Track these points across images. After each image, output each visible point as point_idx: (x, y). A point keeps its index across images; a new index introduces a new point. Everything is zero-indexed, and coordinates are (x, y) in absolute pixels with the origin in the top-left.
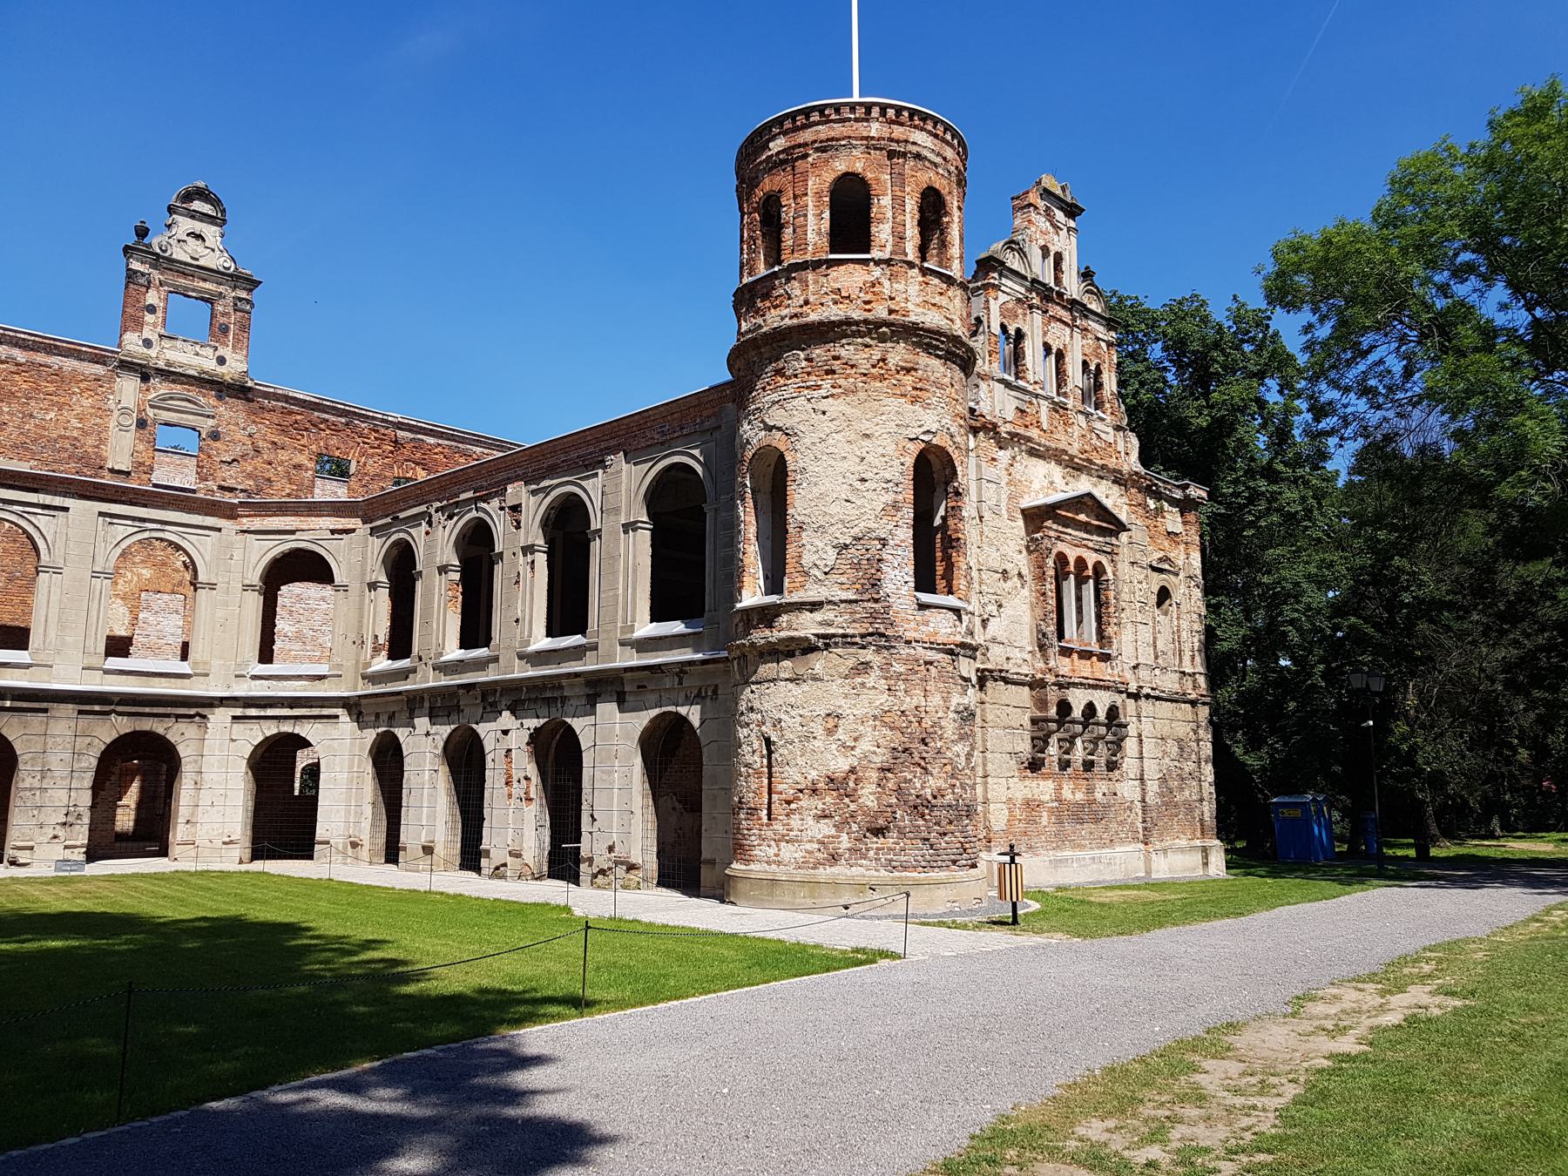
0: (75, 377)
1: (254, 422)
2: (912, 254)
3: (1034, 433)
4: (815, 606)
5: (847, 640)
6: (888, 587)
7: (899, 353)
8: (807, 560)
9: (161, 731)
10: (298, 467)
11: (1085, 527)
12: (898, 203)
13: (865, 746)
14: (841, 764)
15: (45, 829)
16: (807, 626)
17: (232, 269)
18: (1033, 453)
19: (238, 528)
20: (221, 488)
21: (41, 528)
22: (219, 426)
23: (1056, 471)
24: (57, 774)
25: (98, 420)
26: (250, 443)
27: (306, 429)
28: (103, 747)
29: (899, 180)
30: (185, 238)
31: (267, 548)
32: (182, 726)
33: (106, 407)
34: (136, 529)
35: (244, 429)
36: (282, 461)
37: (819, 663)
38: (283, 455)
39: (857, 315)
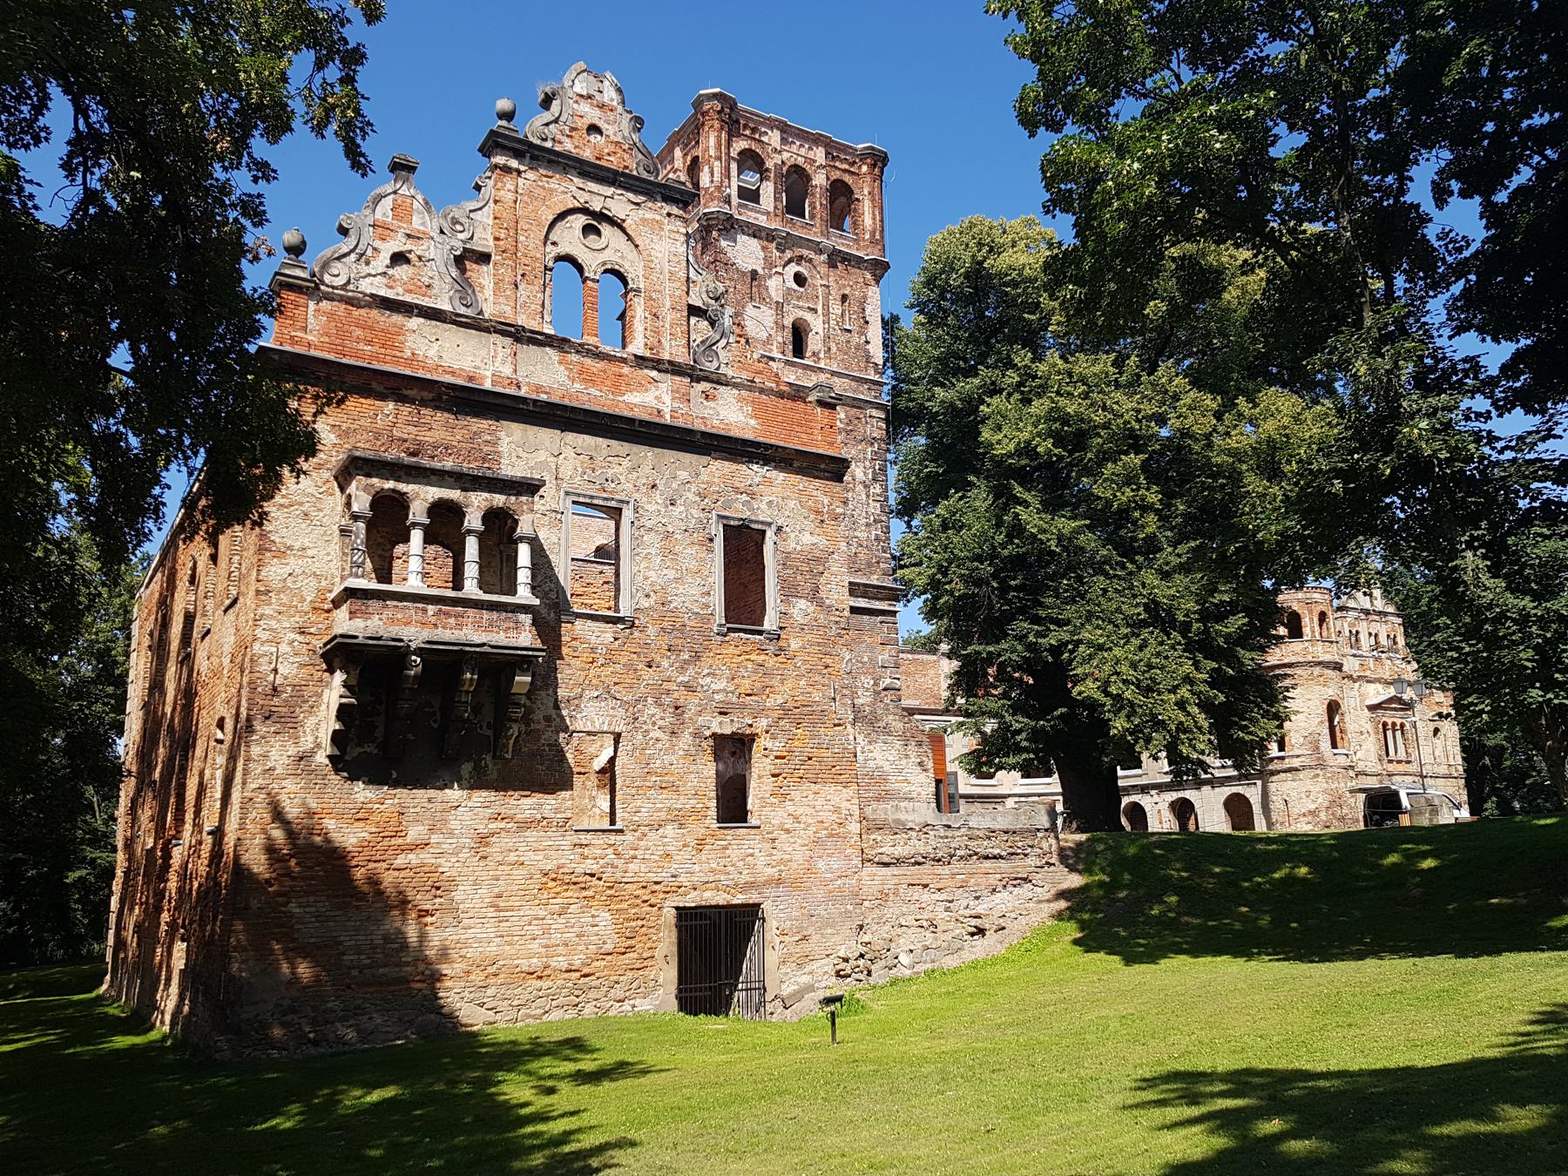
2: (1318, 638)
3: (1368, 673)
4: (1298, 756)
5: (1311, 767)
6: (1322, 749)
7: (1317, 670)
8: (1293, 742)
11: (1395, 709)
12: (1311, 620)
13: (1320, 800)
14: (1313, 807)
16: (1296, 763)
18: (1368, 682)
23: (1379, 687)
29: (1311, 612)
37: (1301, 775)
39: (1301, 660)
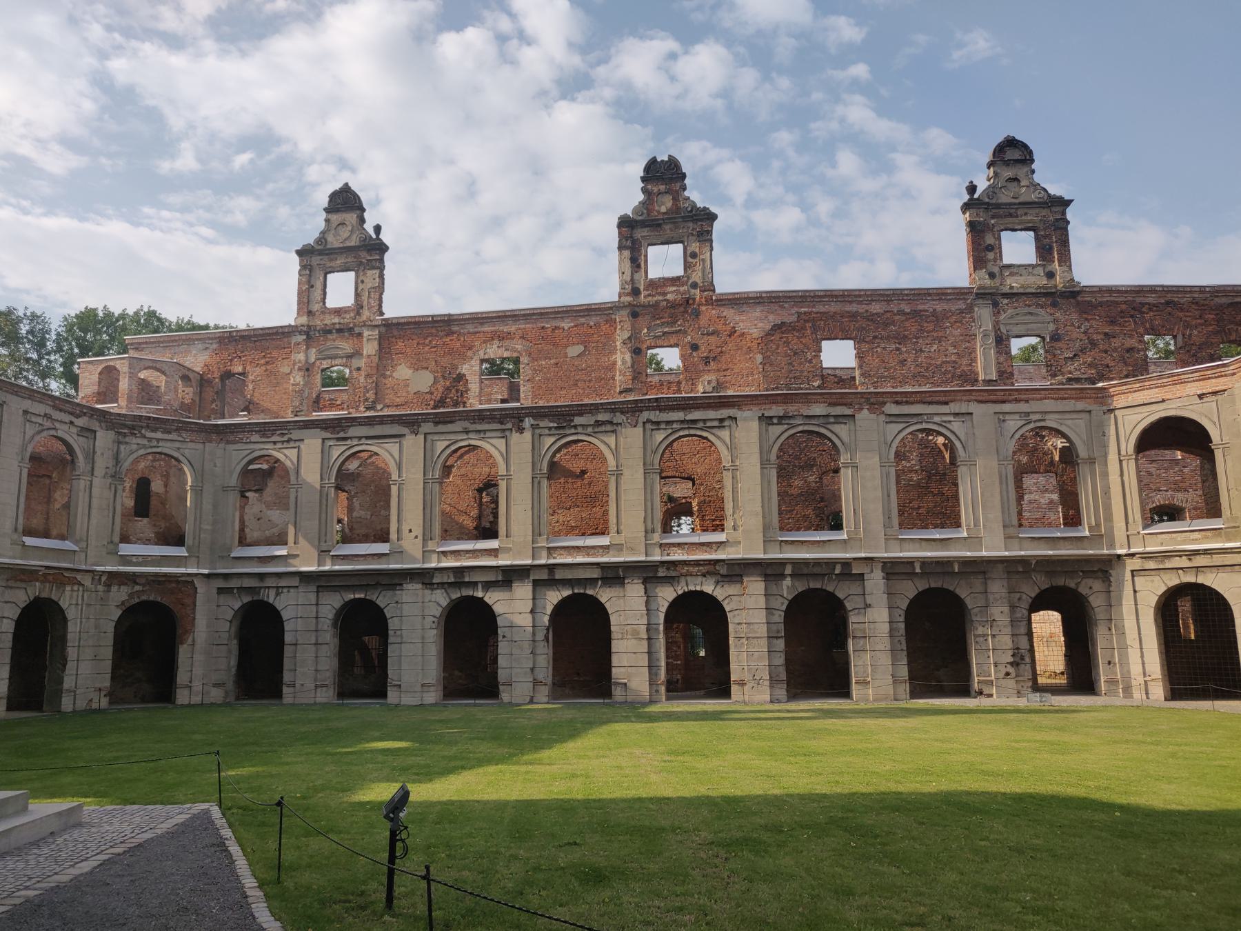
0: (945, 315)
1: (1086, 319)
9: (1072, 585)
10: (1130, 350)
15: (1000, 667)
17: (1046, 198)
19: (1105, 408)
20: (1070, 380)
21: (957, 433)
22: (1057, 329)
24: (1000, 623)
25: (967, 344)
26: (1086, 338)
27: (1132, 316)
28: (1030, 600)
30: (1005, 184)
31: (1135, 423)
32: (1090, 582)
33: (971, 333)
34: (1023, 422)
35: (1079, 327)
36: (1115, 348)
38: (1116, 343)
